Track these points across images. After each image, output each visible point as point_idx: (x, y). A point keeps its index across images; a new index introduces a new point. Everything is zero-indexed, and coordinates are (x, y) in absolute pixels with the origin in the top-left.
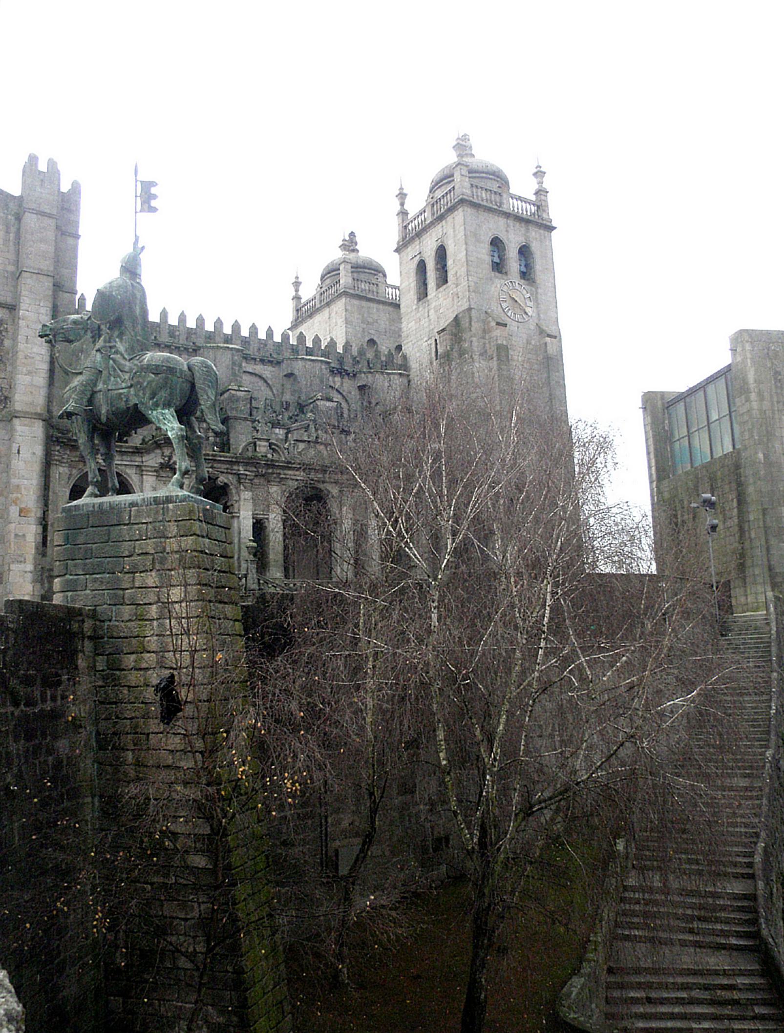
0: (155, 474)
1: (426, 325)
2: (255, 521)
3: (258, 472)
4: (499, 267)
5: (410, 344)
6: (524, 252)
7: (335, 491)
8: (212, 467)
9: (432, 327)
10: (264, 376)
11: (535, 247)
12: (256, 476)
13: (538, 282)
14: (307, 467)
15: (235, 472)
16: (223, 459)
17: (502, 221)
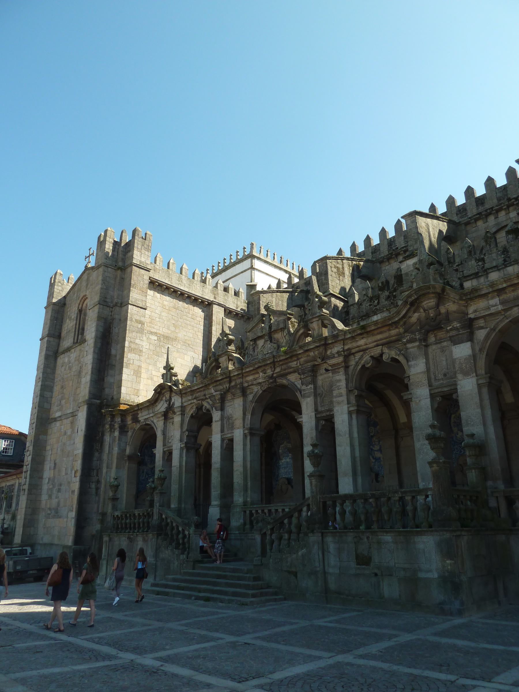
0: (163, 418)
7: (298, 384)
8: (195, 398)
16: (196, 388)
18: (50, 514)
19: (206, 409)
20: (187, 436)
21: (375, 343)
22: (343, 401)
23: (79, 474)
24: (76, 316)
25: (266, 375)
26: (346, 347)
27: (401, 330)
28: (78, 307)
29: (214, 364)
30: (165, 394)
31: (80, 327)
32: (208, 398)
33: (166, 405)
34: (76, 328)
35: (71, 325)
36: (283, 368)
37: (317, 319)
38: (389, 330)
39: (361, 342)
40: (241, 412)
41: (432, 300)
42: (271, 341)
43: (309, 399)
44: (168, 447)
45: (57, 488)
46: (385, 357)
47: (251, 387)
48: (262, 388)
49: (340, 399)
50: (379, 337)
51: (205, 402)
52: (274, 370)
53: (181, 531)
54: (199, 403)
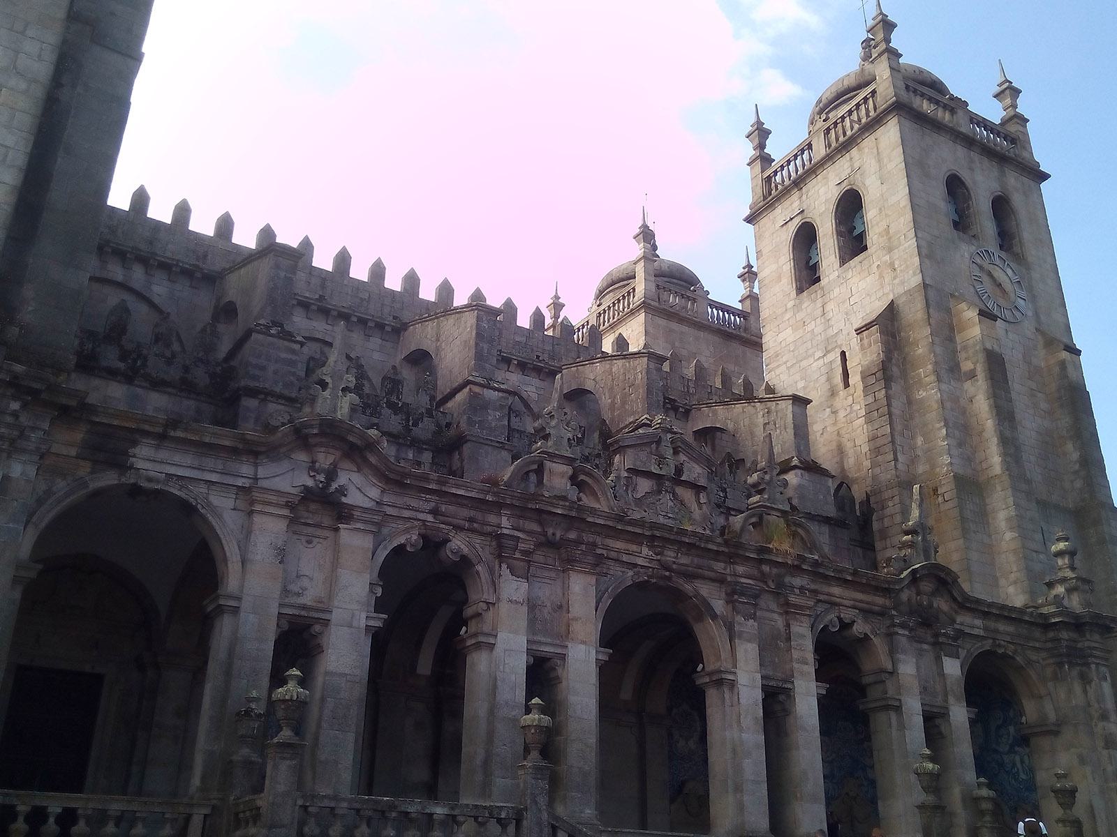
0: (286, 512)
1: (818, 330)
2: (532, 660)
3: (545, 534)
4: (962, 223)
5: (783, 368)
6: (1001, 206)
7: (719, 605)
8: (435, 512)
9: (831, 332)
10: (524, 395)
11: (1017, 200)
12: (539, 545)
13: (1030, 259)
14: (657, 537)
15: (489, 529)
17: (961, 151)
21: (852, 602)
22: (809, 673)
25: (659, 557)
26: (813, 587)
27: (888, 603)
29: (535, 467)
37: (778, 515)
38: (875, 595)
39: (836, 590)
41: (930, 585)
43: (749, 645)
44: (304, 607)
46: (854, 628)
47: (611, 563)
49: (805, 668)
50: (860, 596)
51: (462, 535)
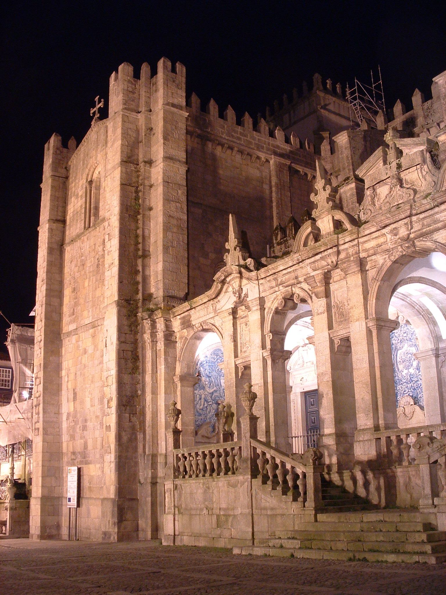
18: (75, 460)
19: (300, 298)
20: (271, 340)
23: (114, 404)
24: (84, 191)
25: (398, 237)
28: (87, 180)
30: (231, 283)
31: (92, 206)
32: (302, 280)
33: (234, 299)
34: (86, 208)
35: (79, 204)
36: (425, 223)
40: (360, 298)
42: (401, 186)
45: (80, 424)
48: (391, 258)
52: (412, 228)
53: (290, 470)
54: (287, 291)
